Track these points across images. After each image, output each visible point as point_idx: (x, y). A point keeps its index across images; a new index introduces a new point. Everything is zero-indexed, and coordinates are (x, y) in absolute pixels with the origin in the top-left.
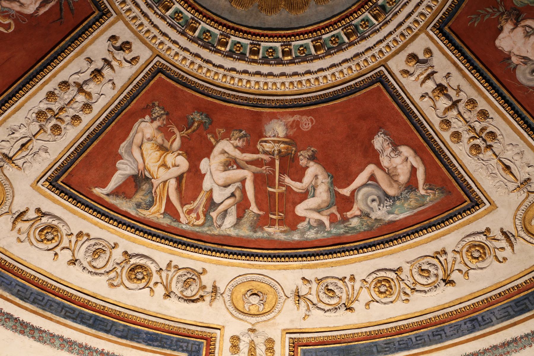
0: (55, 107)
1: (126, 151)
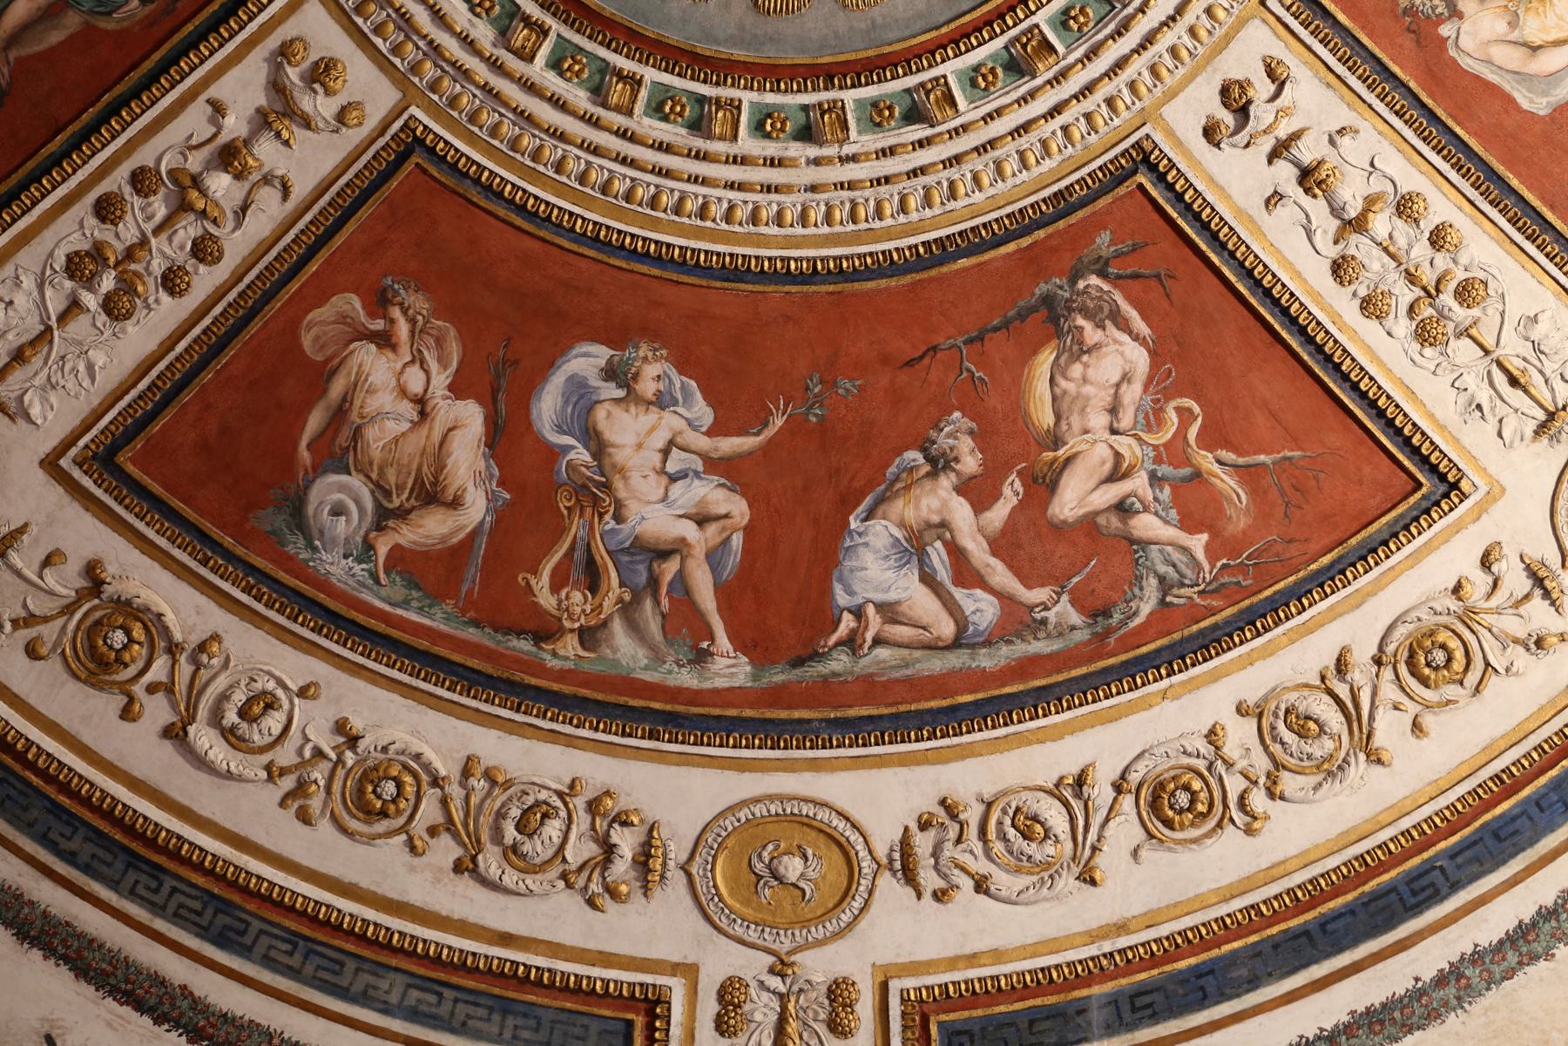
0: (1405, 294)
1: (1545, 94)
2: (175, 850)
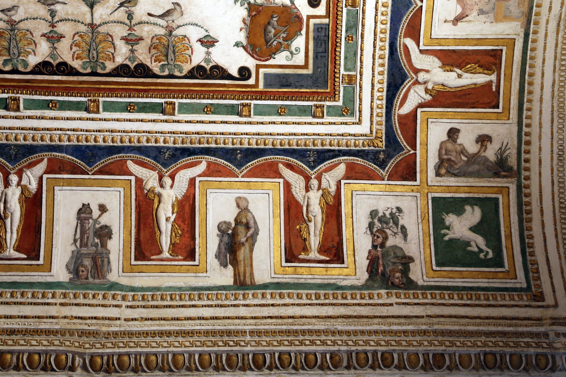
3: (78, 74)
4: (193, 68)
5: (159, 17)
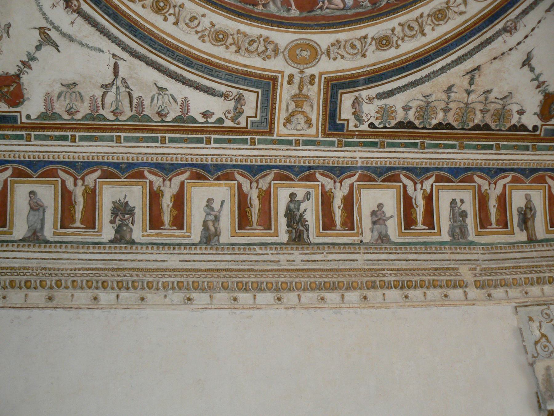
2: (177, 48)
3: (455, 129)
4: (511, 126)
5: (501, 99)
